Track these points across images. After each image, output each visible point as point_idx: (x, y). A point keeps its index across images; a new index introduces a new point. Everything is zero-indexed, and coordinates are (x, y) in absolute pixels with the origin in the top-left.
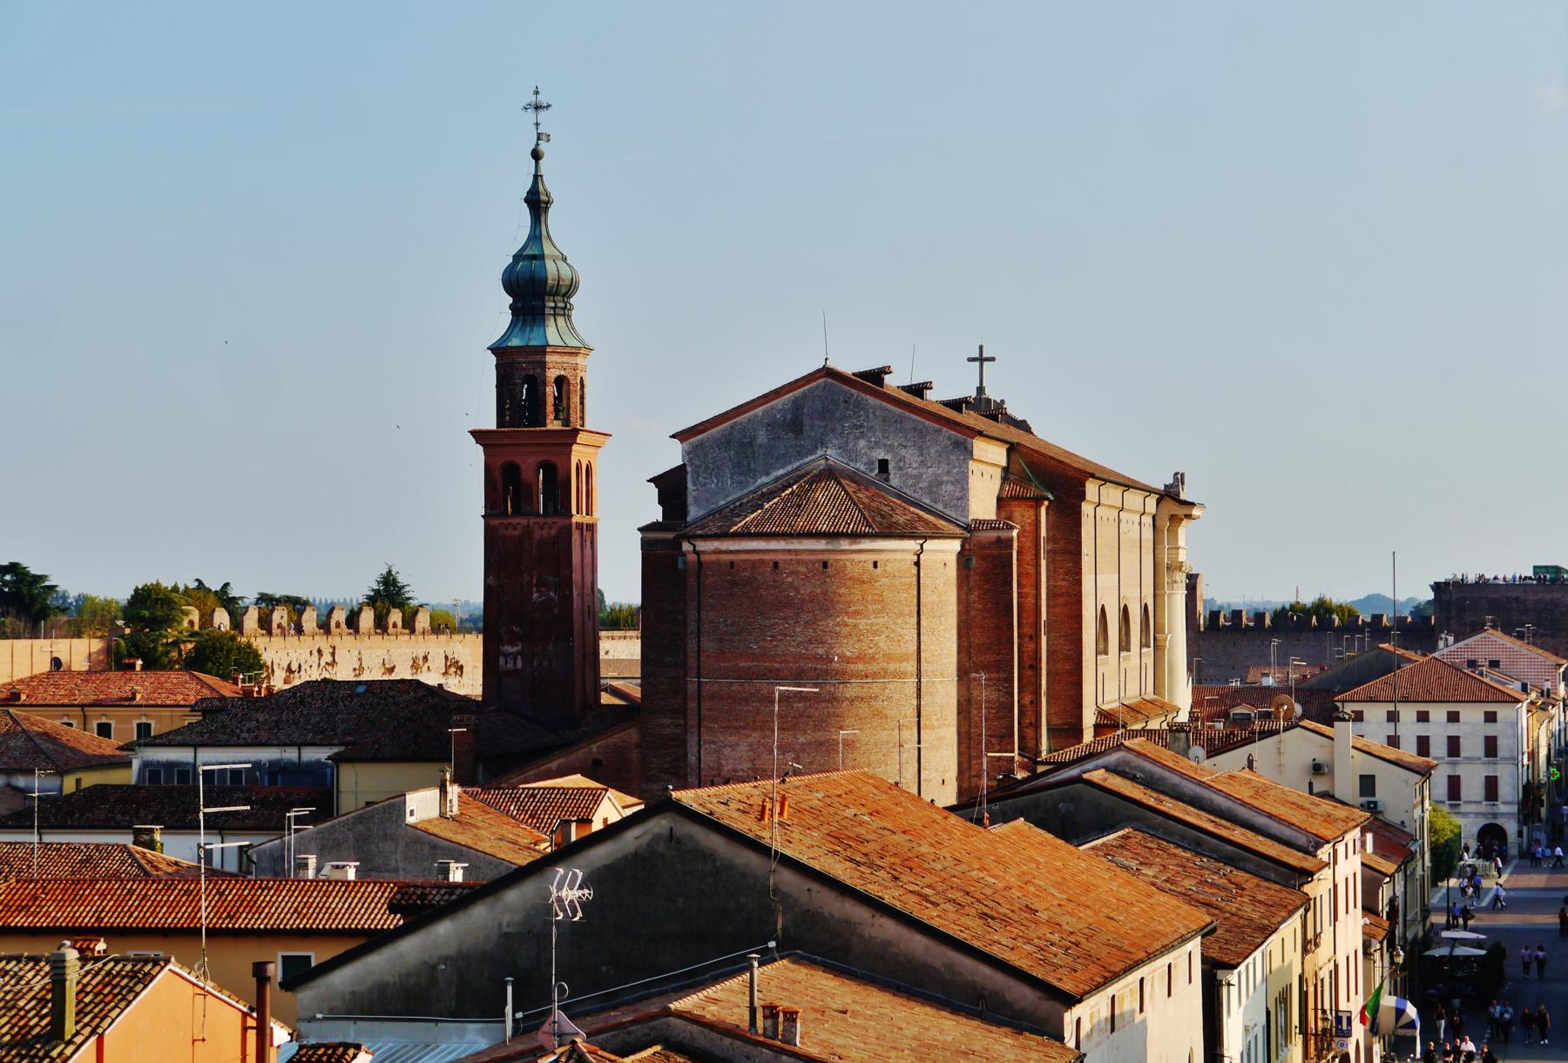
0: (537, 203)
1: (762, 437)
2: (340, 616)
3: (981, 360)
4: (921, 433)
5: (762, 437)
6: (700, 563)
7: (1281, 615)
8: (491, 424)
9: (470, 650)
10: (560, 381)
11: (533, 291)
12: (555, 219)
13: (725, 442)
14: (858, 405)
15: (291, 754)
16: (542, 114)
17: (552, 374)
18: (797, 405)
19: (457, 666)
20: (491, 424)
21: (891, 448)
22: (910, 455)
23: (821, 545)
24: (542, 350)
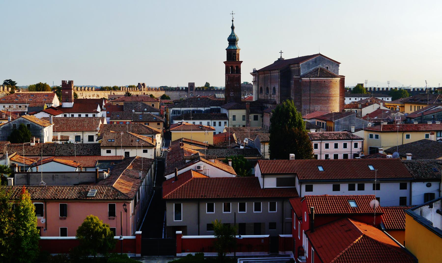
0: (233, 28)
1: (311, 63)
3: (281, 52)
5: (311, 63)
8: (226, 60)
11: (232, 40)
12: (235, 30)
14: (324, 59)
15: (196, 109)
16: (234, 15)
18: (316, 59)
22: (331, 66)
23: (331, 79)
24: (236, 49)
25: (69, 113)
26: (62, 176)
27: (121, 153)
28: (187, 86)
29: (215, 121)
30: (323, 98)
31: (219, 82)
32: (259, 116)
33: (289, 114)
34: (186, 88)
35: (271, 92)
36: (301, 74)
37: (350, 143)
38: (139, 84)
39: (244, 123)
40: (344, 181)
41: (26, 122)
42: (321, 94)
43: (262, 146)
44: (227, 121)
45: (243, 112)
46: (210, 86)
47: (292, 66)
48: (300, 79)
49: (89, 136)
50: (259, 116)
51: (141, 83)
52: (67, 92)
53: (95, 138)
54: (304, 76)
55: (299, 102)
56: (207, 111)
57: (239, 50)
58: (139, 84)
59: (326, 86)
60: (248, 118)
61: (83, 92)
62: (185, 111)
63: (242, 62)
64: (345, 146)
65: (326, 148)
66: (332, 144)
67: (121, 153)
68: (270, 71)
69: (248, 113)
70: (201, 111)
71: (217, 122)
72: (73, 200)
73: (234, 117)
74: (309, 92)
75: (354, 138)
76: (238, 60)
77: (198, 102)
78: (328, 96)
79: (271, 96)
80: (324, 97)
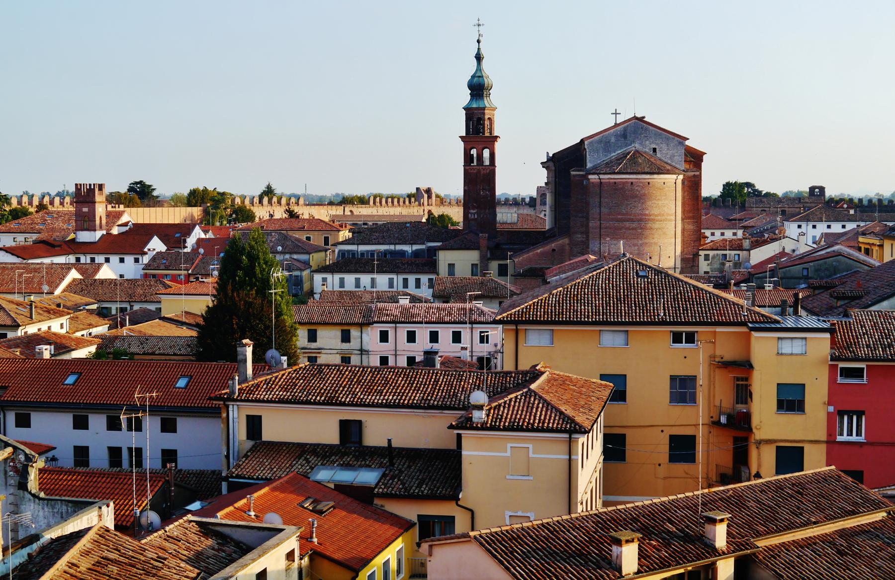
0: (479, 58)
1: (613, 140)
2: (256, 200)
3: (616, 114)
4: (668, 139)
5: (613, 140)
6: (601, 183)
9: (460, 210)
10: (489, 119)
11: (478, 88)
12: (484, 63)
13: (600, 141)
14: (646, 129)
15: (392, 247)
16: (481, 28)
17: (487, 117)
18: (625, 129)
19: (545, 218)
20: (464, 134)
21: (657, 144)
22: (664, 146)
23: (648, 176)
24: (484, 109)
28: (534, 194)
29: (405, 276)
30: (627, 224)
34: (531, 198)
36: (589, 165)
37: (469, 331)
40: (97, 408)
42: (624, 214)
45: (474, 256)
48: (585, 177)
51: (423, 187)
52: (85, 210)
55: (582, 233)
56: (416, 254)
57: (494, 109)
58: (418, 189)
61: (274, 208)
62: (368, 251)
63: (497, 137)
64: (457, 337)
65: (381, 341)
66: (423, 334)
70: (402, 253)
71: (412, 278)
73: (451, 266)
76: (491, 133)
78: (641, 220)
80: (632, 220)
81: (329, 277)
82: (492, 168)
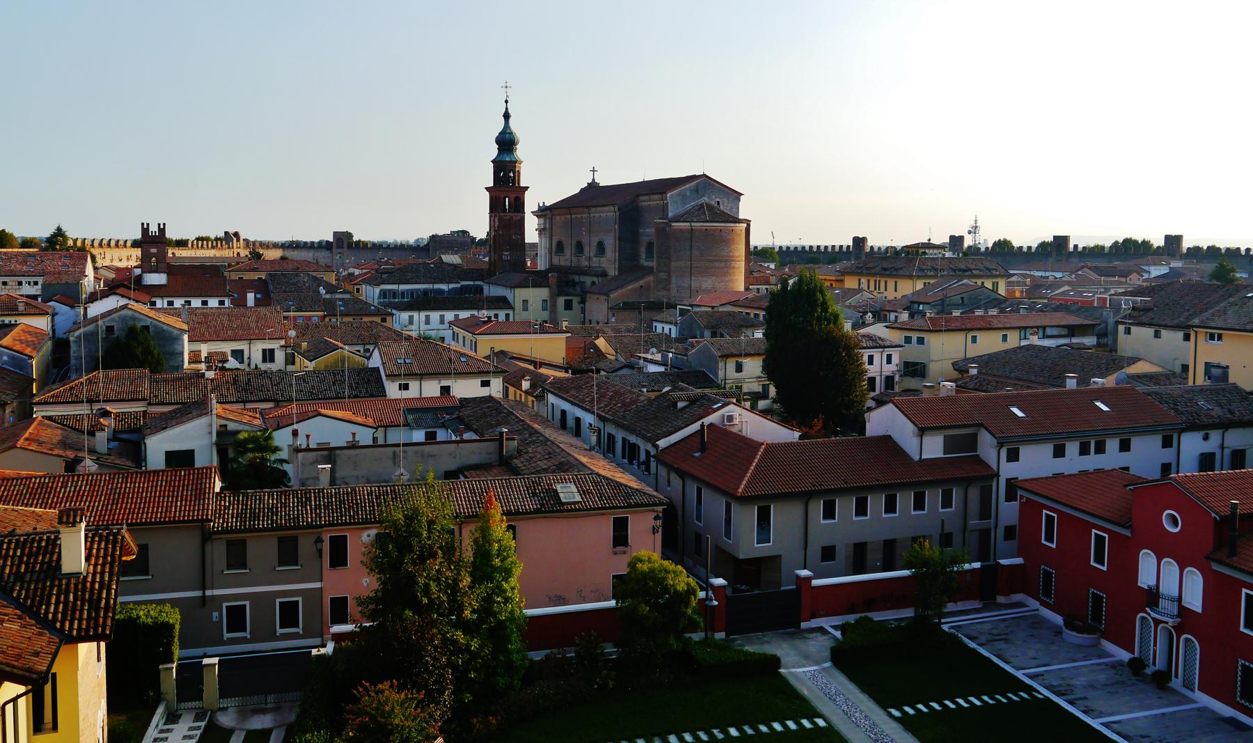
0: (507, 116)
7: (320, 243)
8: (491, 184)
11: (506, 142)
12: (511, 121)
15: (430, 286)
18: (697, 185)
25: (162, 297)
26: (416, 453)
27: (431, 389)
30: (717, 264)
31: (480, 227)
32: (575, 300)
33: (815, 295)
34: (328, 242)
35: (591, 250)
36: (670, 214)
38: (226, 233)
39: (546, 315)
41: (140, 320)
43: (721, 365)
44: (511, 312)
45: (543, 293)
46: (355, 239)
47: (641, 198)
49: (264, 351)
50: (575, 300)
51: (231, 231)
53: (280, 356)
54: (678, 219)
58: (226, 233)
59: (724, 240)
60: (554, 305)
67: (431, 389)
68: (588, 207)
69: (554, 296)
70: (441, 292)
72: (531, 513)
73: (525, 302)
74: (688, 253)
75: (887, 344)
77: (429, 271)
79: (590, 259)
81: (415, 314)
82: (516, 216)
